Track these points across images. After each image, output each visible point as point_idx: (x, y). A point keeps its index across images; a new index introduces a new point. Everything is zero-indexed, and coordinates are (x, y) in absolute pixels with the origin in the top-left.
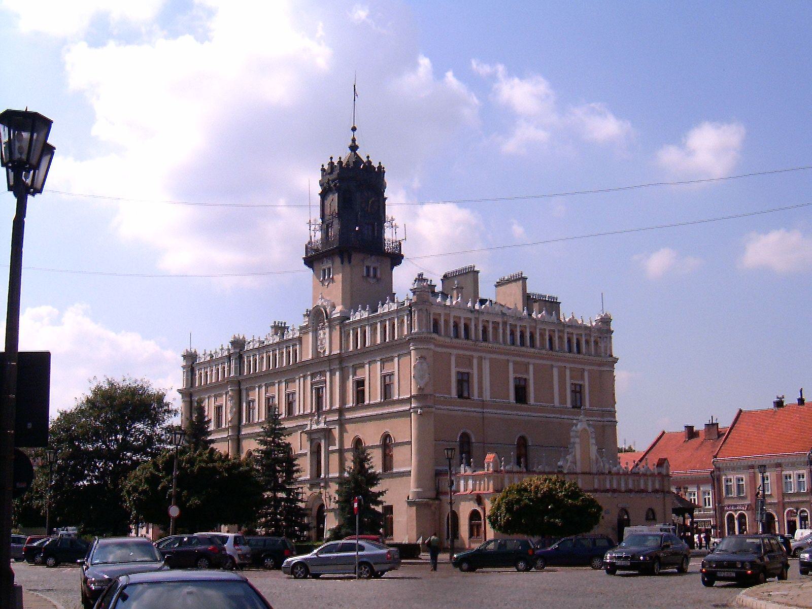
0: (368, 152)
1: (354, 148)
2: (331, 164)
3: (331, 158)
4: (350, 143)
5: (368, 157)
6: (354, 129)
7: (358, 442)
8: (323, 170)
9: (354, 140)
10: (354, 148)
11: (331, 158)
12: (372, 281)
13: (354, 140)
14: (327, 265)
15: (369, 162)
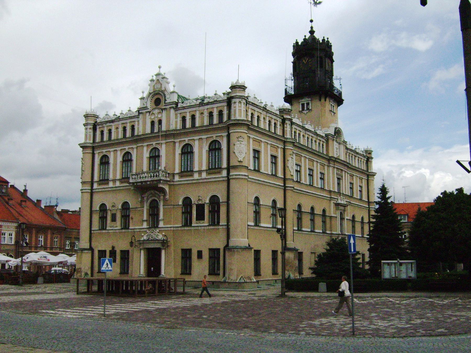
0: (319, 36)
1: (312, 32)
2: (305, 39)
3: (305, 36)
4: (310, 29)
5: (328, 39)
6: (311, 21)
7: (103, 208)
8: (297, 43)
9: (312, 28)
10: (312, 32)
11: (305, 36)
12: (333, 114)
13: (312, 28)
14: (305, 101)
15: (328, 41)
